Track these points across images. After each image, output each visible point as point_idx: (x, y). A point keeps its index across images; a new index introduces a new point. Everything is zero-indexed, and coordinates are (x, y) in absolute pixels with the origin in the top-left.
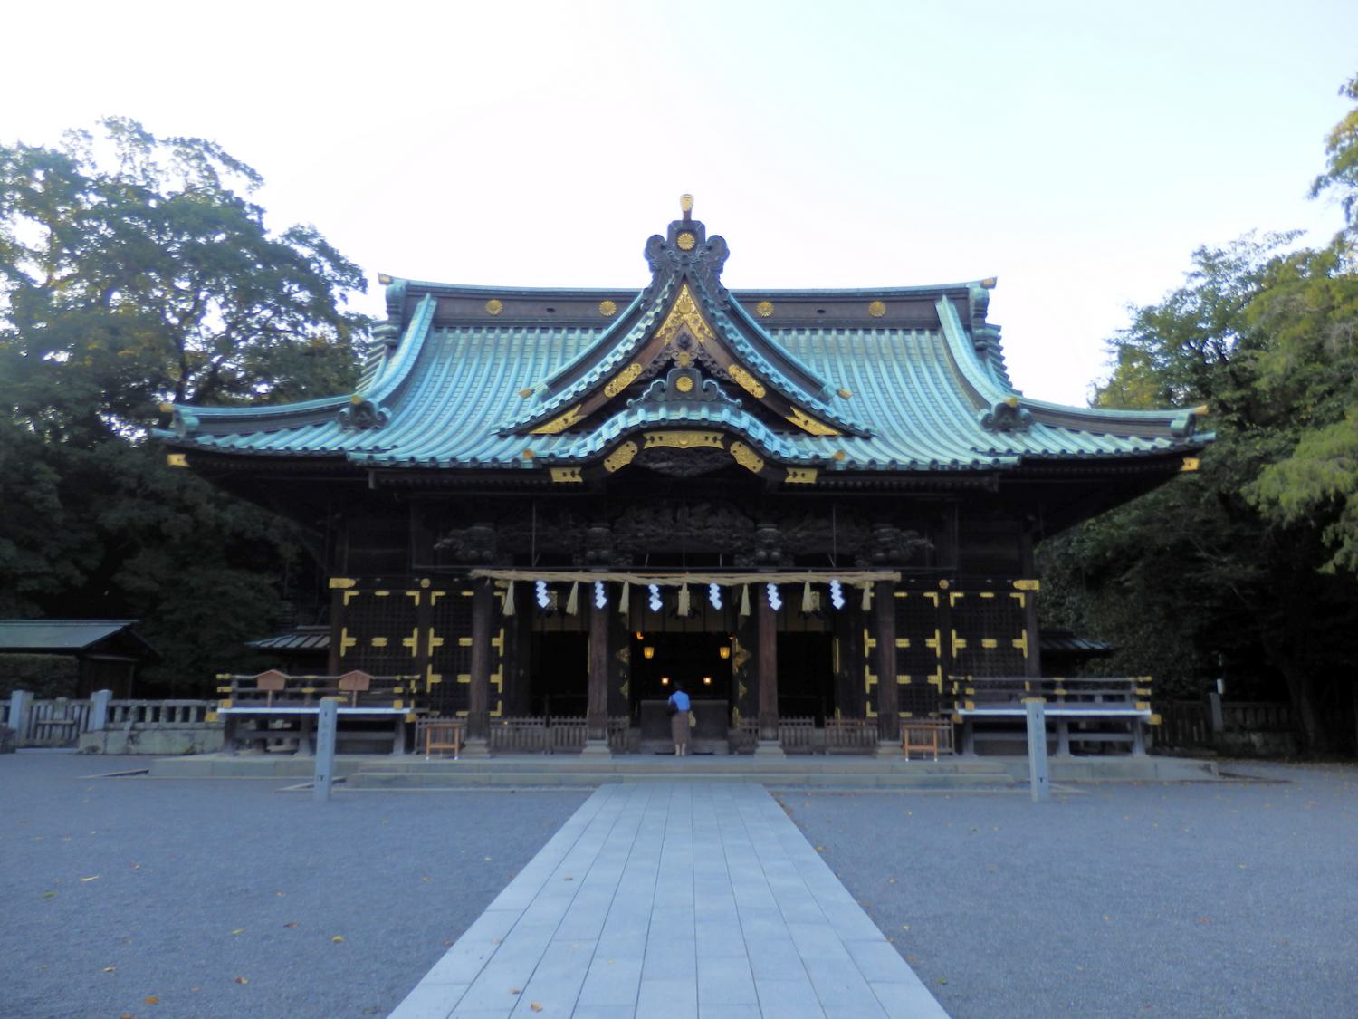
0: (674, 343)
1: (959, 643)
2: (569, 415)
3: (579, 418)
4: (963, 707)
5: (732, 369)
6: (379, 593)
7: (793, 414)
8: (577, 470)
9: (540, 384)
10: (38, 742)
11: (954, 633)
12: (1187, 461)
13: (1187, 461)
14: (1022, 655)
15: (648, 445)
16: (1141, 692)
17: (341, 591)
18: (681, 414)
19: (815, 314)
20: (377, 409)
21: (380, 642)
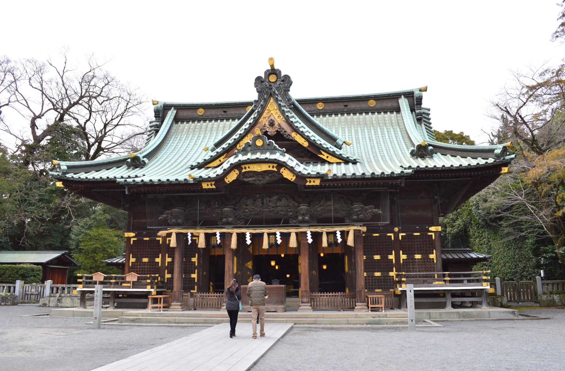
0: (267, 123)
1: (403, 257)
4: (401, 287)
5: (293, 134)
6: (145, 239)
7: (321, 154)
8: (213, 183)
9: (211, 145)
10: (26, 301)
11: (401, 252)
12: (503, 168)
13: (503, 168)
14: (433, 262)
15: (244, 171)
16: (485, 278)
17: (129, 238)
18: (258, 155)
19: (343, 107)
20: (142, 159)
21: (145, 260)
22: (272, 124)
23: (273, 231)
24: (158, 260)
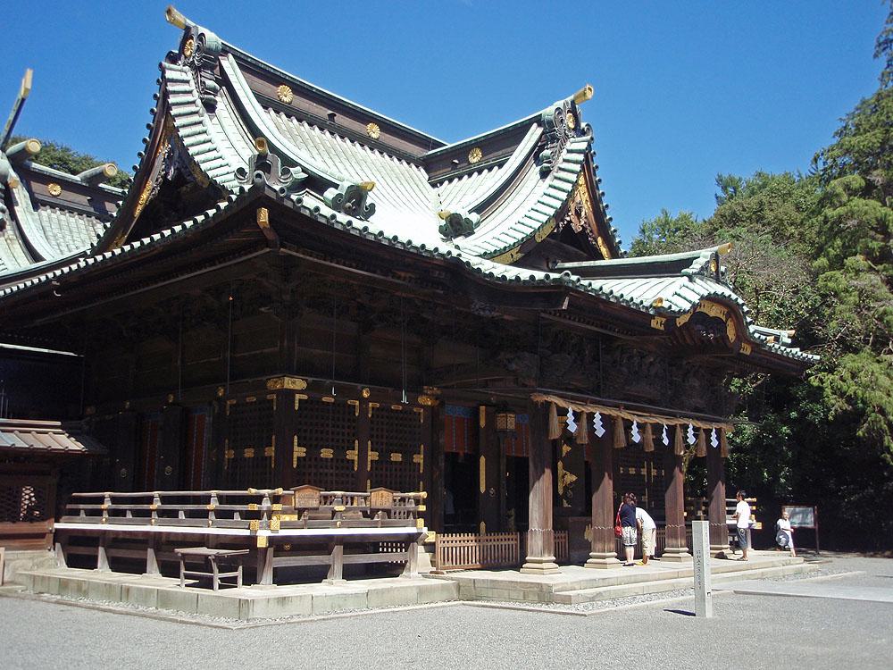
2: (514, 252)
3: (520, 255)
8: (664, 320)
15: (697, 310)
17: (292, 392)
24: (353, 455)
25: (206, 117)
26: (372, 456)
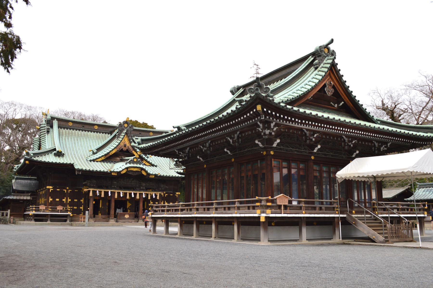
5: (133, 152)
17: (49, 189)
22: (125, 146)
23: (131, 192)
24: (64, 200)
25: (46, 135)
26: (69, 200)
